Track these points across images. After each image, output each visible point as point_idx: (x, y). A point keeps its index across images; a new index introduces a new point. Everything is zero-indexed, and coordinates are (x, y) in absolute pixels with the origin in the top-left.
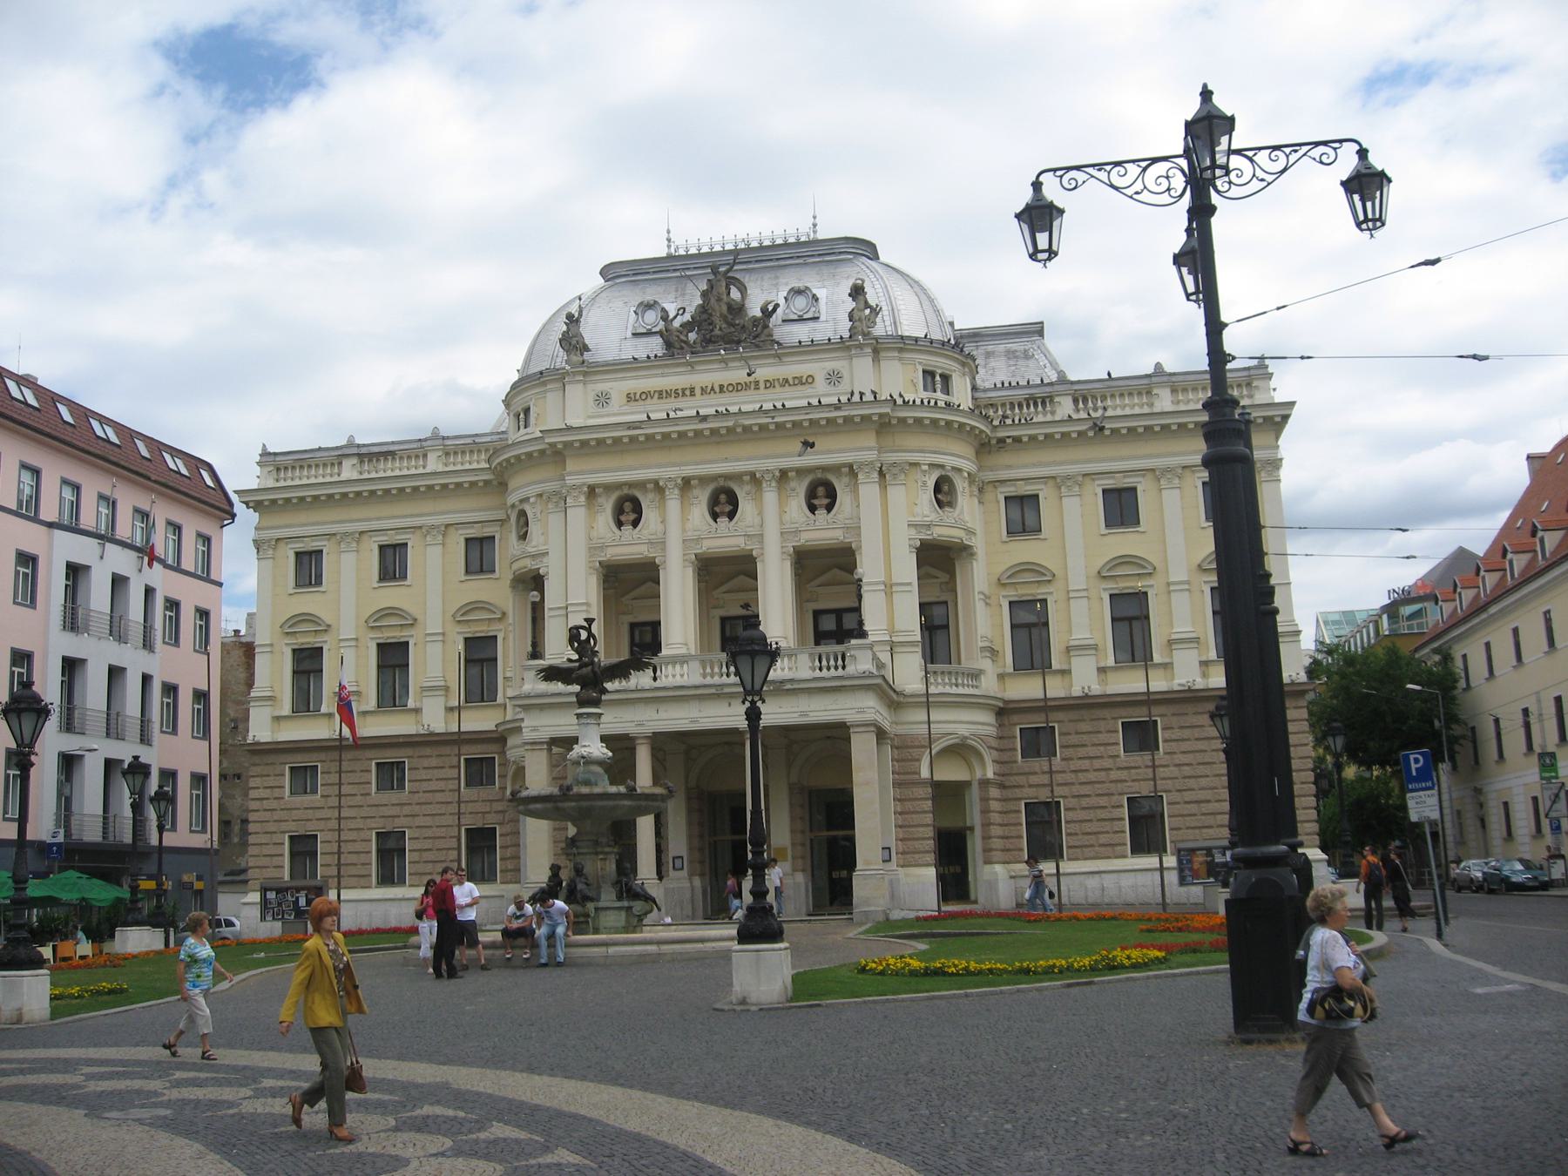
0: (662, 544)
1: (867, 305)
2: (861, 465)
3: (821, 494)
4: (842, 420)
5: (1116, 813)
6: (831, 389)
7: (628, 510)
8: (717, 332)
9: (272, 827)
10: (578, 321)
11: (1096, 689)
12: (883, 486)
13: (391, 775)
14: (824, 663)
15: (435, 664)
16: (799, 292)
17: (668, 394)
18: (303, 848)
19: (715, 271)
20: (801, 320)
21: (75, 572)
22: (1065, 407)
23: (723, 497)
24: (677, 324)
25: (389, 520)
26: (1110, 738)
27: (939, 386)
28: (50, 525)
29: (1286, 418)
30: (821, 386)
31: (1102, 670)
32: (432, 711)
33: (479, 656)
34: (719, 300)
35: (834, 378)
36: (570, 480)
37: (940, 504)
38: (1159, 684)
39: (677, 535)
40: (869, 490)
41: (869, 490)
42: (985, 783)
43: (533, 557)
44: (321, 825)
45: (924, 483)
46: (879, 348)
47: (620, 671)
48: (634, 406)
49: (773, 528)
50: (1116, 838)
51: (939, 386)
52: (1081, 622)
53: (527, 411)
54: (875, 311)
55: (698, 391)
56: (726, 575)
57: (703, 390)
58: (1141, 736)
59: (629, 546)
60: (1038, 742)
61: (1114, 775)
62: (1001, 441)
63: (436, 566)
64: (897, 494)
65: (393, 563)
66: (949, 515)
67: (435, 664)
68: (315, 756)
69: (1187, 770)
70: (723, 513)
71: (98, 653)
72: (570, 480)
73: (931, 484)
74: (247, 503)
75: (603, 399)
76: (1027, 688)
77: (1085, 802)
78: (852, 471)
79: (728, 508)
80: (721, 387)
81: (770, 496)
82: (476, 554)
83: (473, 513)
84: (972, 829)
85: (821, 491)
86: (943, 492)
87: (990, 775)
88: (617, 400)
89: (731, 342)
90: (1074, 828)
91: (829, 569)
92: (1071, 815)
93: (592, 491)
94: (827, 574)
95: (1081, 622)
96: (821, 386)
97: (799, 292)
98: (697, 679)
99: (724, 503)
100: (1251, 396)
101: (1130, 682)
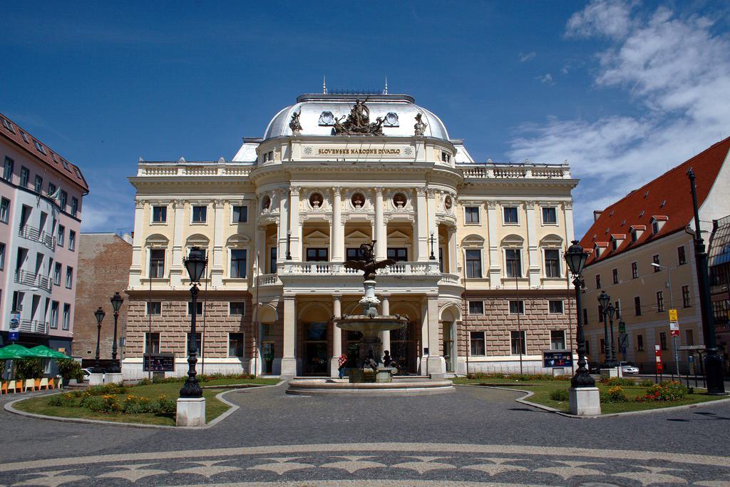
0: (333, 215)
1: (422, 123)
2: (420, 189)
5: (506, 338)
6: (407, 156)
8: (358, 127)
9: (137, 329)
10: (298, 116)
11: (502, 287)
12: (427, 201)
14: (399, 269)
15: (220, 260)
16: (391, 115)
17: (337, 151)
18: (153, 338)
19: (358, 101)
20: (392, 126)
21: (26, 210)
22: (491, 174)
23: (358, 197)
24: (341, 122)
25: (200, 198)
26: (505, 307)
27: (447, 159)
28: (15, 187)
29: (575, 186)
30: (402, 154)
31: (503, 281)
32: (179, 282)
33: (240, 261)
34: (359, 114)
35: (408, 151)
37: (448, 208)
38: (523, 286)
40: (421, 200)
42: (459, 323)
43: (273, 216)
44: (163, 329)
45: (442, 199)
46: (429, 142)
47: (382, 265)
48: (321, 155)
50: (506, 348)
51: (447, 159)
52: (494, 260)
53: (271, 153)
54: (425, 126)
55: (350, 152)
56: (357, 229)
57: (352, 151)
58: (517, 307)
60: (476, 307)
61: (507, 322)
62: (467, 185)
67: (220, 260)
69: (534, 322)
70: (358, 204)
71: (33, 249)
72: (293, 184)
73: (444, 198)
74: (132, 183)
76: (472, 286)
77: (494, 332)
78: (414, 189)
79: (360, 202)
80: (360, 150)
81: (380, 199)
82: (238, 215)
84: (453, 342)
86: (448, 204)
87: (461, 320)
89: (363, 131)
90: (490, 343)
91: (396, 230)
92: (489, 338)
94: (403, 231)
95: (494, 260)
97: (391, 115)
98: (300, 273)
100: (562, 176)
101: (511, 286)
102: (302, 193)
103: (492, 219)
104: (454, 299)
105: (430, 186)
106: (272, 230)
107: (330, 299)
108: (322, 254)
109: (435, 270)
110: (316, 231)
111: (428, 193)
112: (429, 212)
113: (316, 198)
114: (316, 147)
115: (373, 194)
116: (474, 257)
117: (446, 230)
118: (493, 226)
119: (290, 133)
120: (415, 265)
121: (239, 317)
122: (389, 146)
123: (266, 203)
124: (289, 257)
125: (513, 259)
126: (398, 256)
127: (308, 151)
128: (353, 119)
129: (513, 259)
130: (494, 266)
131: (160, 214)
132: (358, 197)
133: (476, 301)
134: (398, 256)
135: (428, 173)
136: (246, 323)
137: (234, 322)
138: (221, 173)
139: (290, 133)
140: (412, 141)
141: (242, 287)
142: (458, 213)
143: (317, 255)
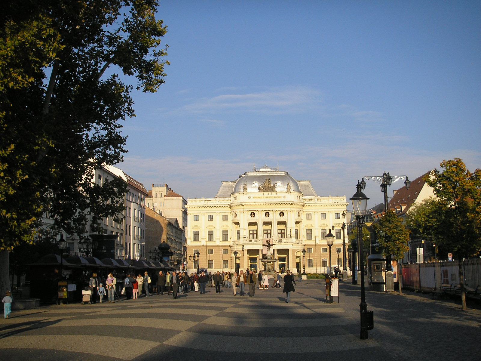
0: (259, 220)
3: (282, 214)
4: (285, 203)
7: (253, 214)
33: (225, 235)
36: (245, 210)
39: (260, 218)
40: (289, 213)
41: (289, 213)
49: (275, 218)
59: (253, 220)
63: (218, 218)
64: (292, 214)
65: (211, 218)
66: (299, 217)
67: (218, 235)
68: (198, 248)
72: (245, 210)
75: (250, 198)
85: (282, 213)
88: (252, 198)
96: (282, 198)
99: (267, 214)
108: (255, 232)
109: (293, 239)
114: (252, 195)
122: (279, 195)
124: (245, 238)
127: (250, 198)
130: (317, 235)
131: (196, 218)
132: (267, 213)
138: (217, 203)
142: (304, 217)
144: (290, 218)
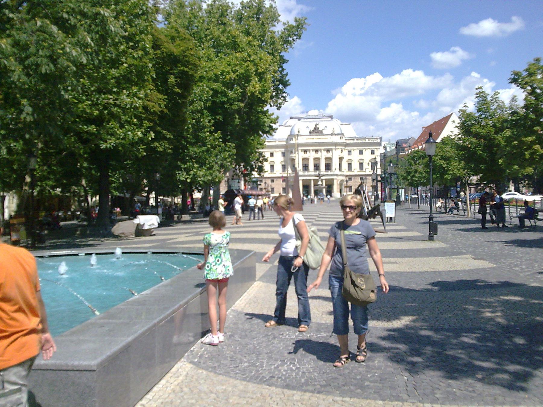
13: (273, 181)
33: (284, 167)
39: (312, 155)
40: (334, 150)
52: (355, 166)
78: (332, 149)
81: (323, 151)
83: (283, 150)
93: (302, 150)
95: (355, 166)
102: (302, 150)
103: (355, 153)
104: (344, 178)
105: (337, 147)
106: (293, 160)
107: (310, 180)
110: (305, 160)
111: (336, 149)
112: (336, 155)
113: (305, 151)
115: (321, 150)
116: (350, 165)
117: (341, 159)
118: (355, 156)
119: (298, 133)
120: (331, 171)
121: (284, 183)
123: (292, 152)
125: (361, 165)
126: (328, 167)
128: (315, 129)
129: (361, 165)
133: (350, 178)
134: (328, 167)
135: (336, 144)
136: (287, 185)
137: (284, 184)
139: (298, 133)
140: (332, 134)
141: (285, 175)
142: (345, 153)
143: (306, 167)
144: (336, 155)
